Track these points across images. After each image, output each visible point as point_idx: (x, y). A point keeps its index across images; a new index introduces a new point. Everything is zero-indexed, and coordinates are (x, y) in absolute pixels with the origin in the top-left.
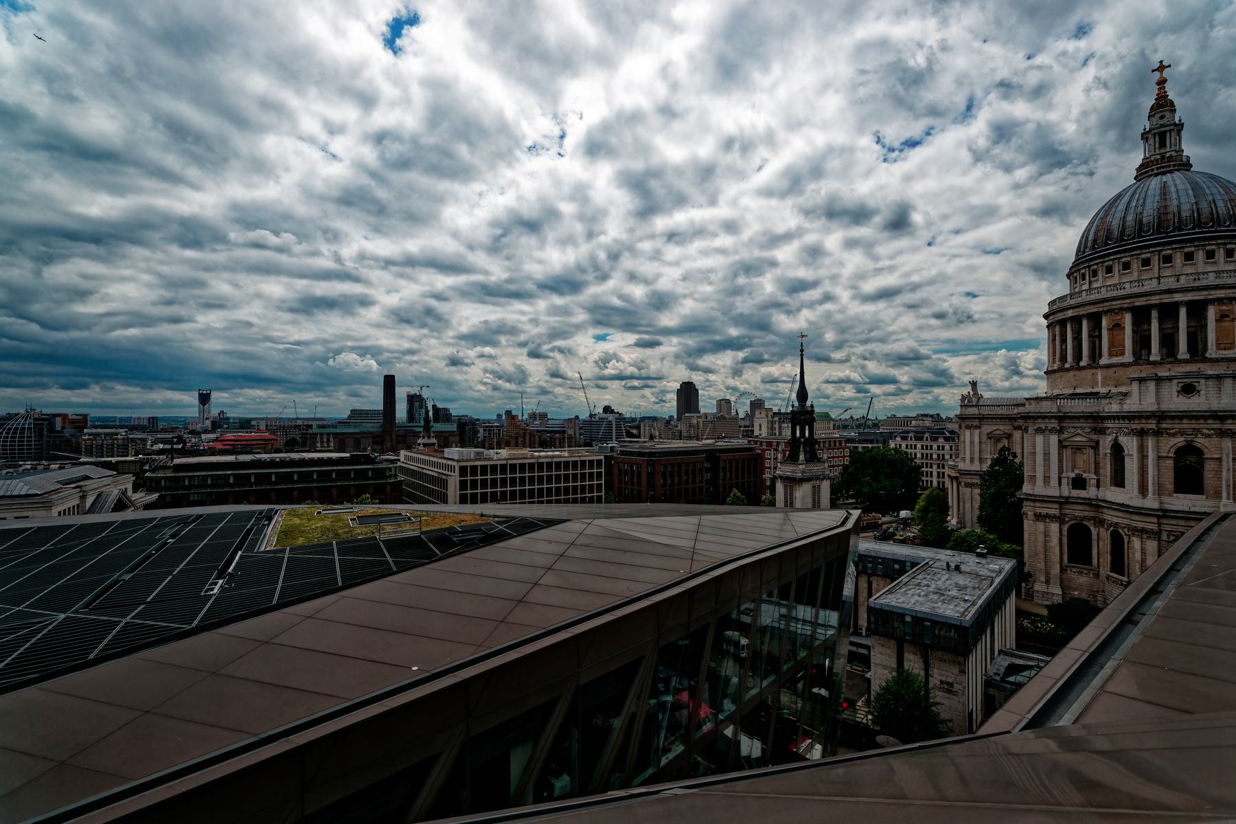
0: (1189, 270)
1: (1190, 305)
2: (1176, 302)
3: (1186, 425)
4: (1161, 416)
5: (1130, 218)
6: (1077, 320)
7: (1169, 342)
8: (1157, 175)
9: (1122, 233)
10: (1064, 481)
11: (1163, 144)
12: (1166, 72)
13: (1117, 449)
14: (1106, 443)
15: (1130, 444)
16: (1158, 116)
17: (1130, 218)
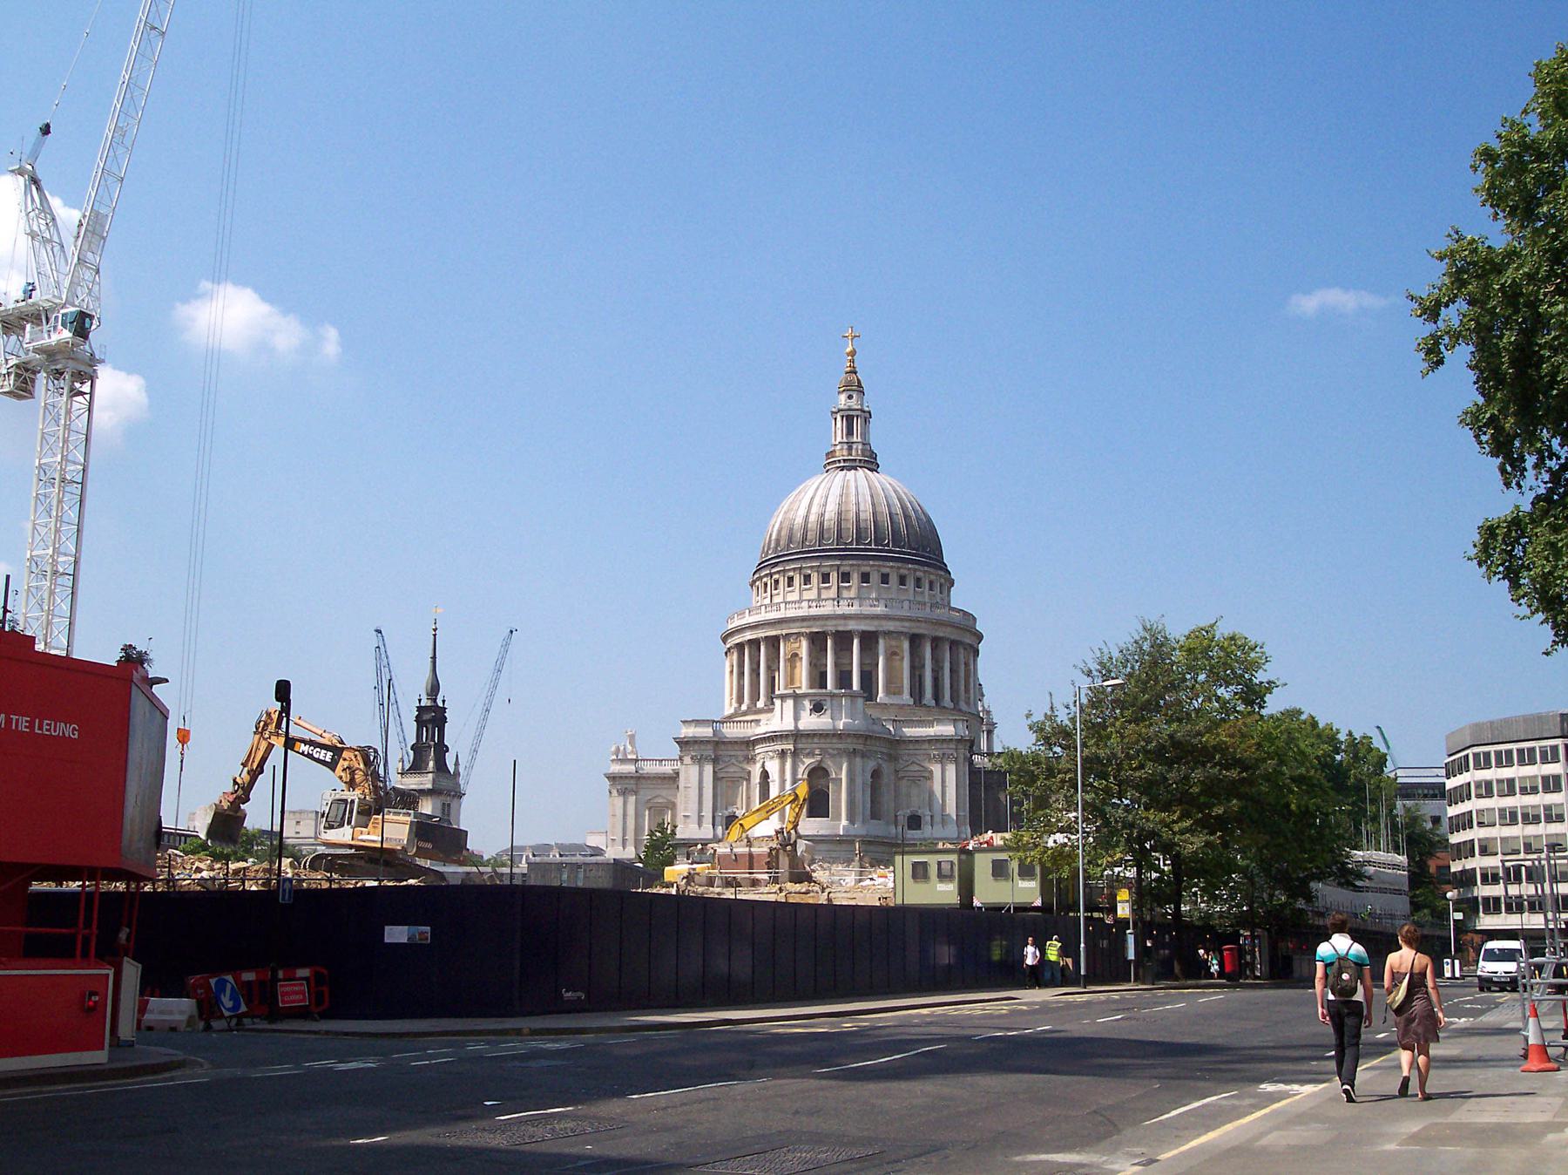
3: (815, 745)
4: (797, 735)
5: (813, 518)
6: (755, 644)
7: (844, 679)
9: (804, 539)
10: (718, 820)
11: (850, 432)
13: (765, 775)
14: (756, 771)
15: (773, 767)
17: (813, 518)
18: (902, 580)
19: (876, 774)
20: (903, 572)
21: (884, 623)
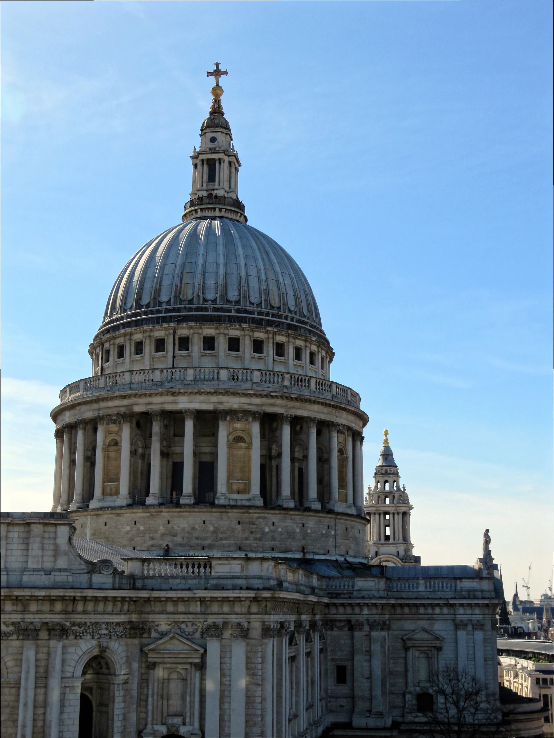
0: (208, 362)
1: (200, 416)
2: (180, 412)
8: (203, 218)
11: (212, 178)
12: (223, 80)
16: (209, 135)
18: (258, 346)
19: (98, 664)
20: (260, 335)
21: (225, 399)
